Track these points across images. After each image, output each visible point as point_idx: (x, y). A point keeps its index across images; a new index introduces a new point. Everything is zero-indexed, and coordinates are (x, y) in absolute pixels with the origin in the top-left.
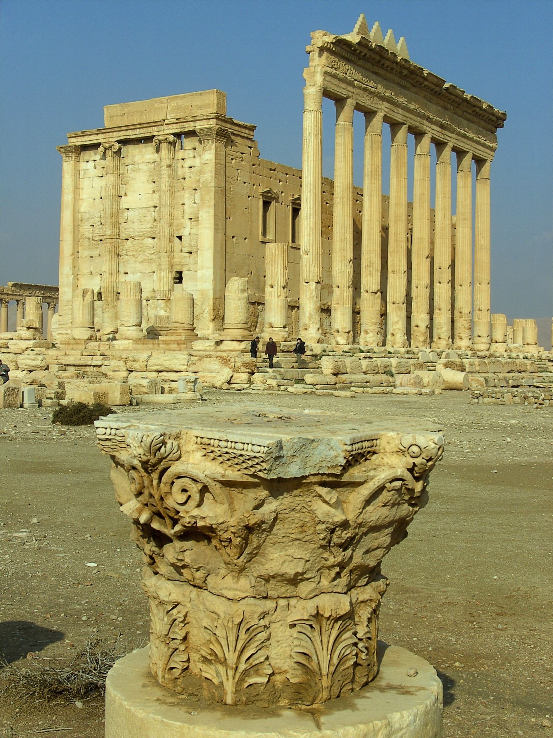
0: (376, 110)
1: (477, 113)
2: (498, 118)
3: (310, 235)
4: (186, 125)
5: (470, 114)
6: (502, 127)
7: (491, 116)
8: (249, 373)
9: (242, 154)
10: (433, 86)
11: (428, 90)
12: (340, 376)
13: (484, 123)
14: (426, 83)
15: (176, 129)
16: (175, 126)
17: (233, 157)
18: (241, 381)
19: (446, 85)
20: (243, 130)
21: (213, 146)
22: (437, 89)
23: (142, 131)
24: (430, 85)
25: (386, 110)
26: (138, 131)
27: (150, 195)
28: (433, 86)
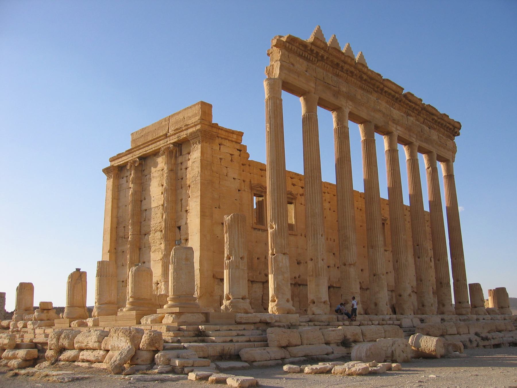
0: (340, 106)
1: (436, 121)
2: (455, 127)
3: (275, 209)
4: (182, 133)
5: (430, 121)
6: (459, 135)
7: (448, 125)
8: (153, 351)
9: (231, 155)
10: (393, 93)
11: (390, 97)
12: (290, 349)
13: (443, 131)
14: (386, 89)
15: (174, 139)
16: (174, 137)
17: (221, 157)
18: (143, 361)
19: (404, 92)
20: (231, 135)
21: (199, 146)
22: (397, 95)
23: (153, 146)
24: (390, 91)
25: (351, 107)
26: (150, 147)
27: (159, 196)
28: (393, 93)
